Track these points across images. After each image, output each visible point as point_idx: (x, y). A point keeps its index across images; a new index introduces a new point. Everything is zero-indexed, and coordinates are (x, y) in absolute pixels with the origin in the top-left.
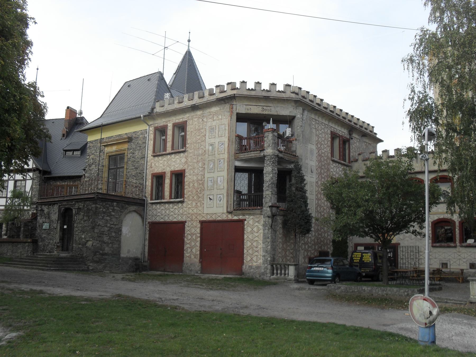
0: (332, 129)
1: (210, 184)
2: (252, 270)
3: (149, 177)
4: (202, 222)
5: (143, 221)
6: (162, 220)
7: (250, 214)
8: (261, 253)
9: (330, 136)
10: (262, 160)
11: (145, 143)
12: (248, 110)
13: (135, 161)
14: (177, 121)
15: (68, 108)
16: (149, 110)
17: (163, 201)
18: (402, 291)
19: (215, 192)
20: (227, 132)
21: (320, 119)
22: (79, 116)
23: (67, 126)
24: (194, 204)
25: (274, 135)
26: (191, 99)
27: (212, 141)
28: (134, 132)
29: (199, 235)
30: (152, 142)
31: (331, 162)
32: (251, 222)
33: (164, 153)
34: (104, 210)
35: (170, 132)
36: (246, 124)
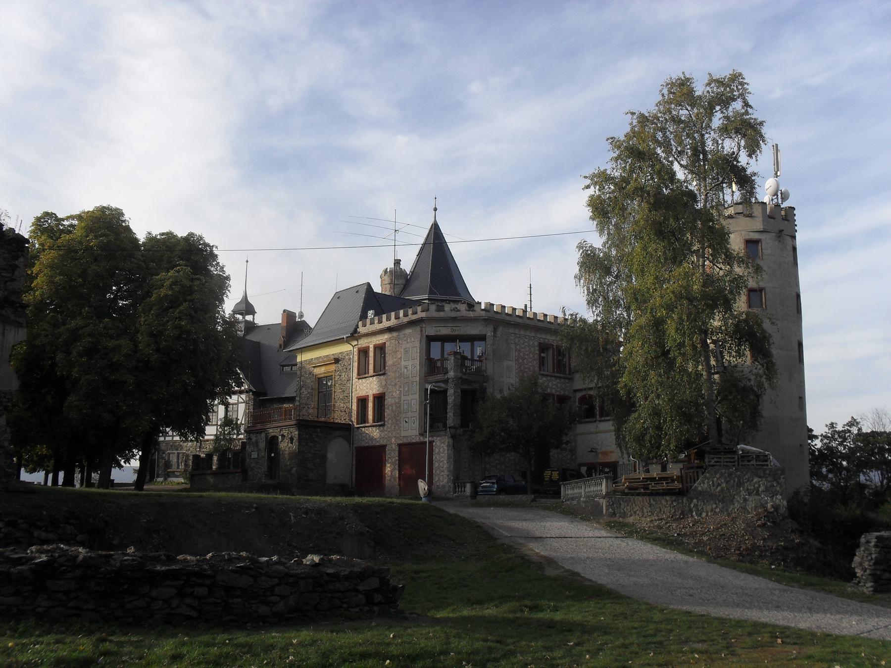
0: (541, 340)
1: (406, 407)
2: (439, 490)
3: (355, 401)
4: (400, 445)
5: (350, 446)
6: (367, 445)
7: (437, 436)
8: (446, 473)
9: (538, 348)
10: (446, 381)
11: (350, 364)
12: (437, 331)
13: (342, 384)
14: (377, 342)
15: (284, 311)
16: (352, 330)
17: (367, 425)
18: (524, 497)
19: (410, 414)
20: (418, 354)
21: (522, 332)
22: (299, 320)
23: (284, 335)
24: (393, 427)
25: (455, 358)
26: (388, 319)
27: (406, 363)
28: (340, 353)
29: (397, 458)
30: (356, 364)
31: (540, 377)
32: (438, 443)
33: (367, 375)
34: (307, 436)
35: (371, 354)
36: (440, 343)
